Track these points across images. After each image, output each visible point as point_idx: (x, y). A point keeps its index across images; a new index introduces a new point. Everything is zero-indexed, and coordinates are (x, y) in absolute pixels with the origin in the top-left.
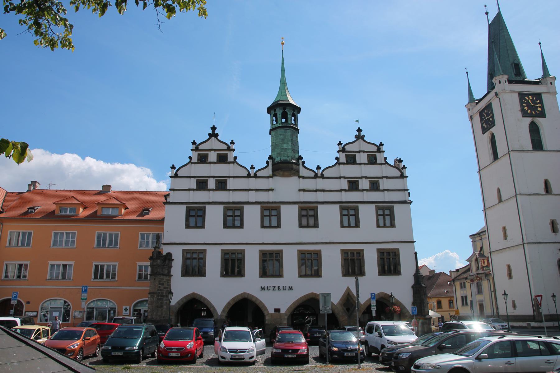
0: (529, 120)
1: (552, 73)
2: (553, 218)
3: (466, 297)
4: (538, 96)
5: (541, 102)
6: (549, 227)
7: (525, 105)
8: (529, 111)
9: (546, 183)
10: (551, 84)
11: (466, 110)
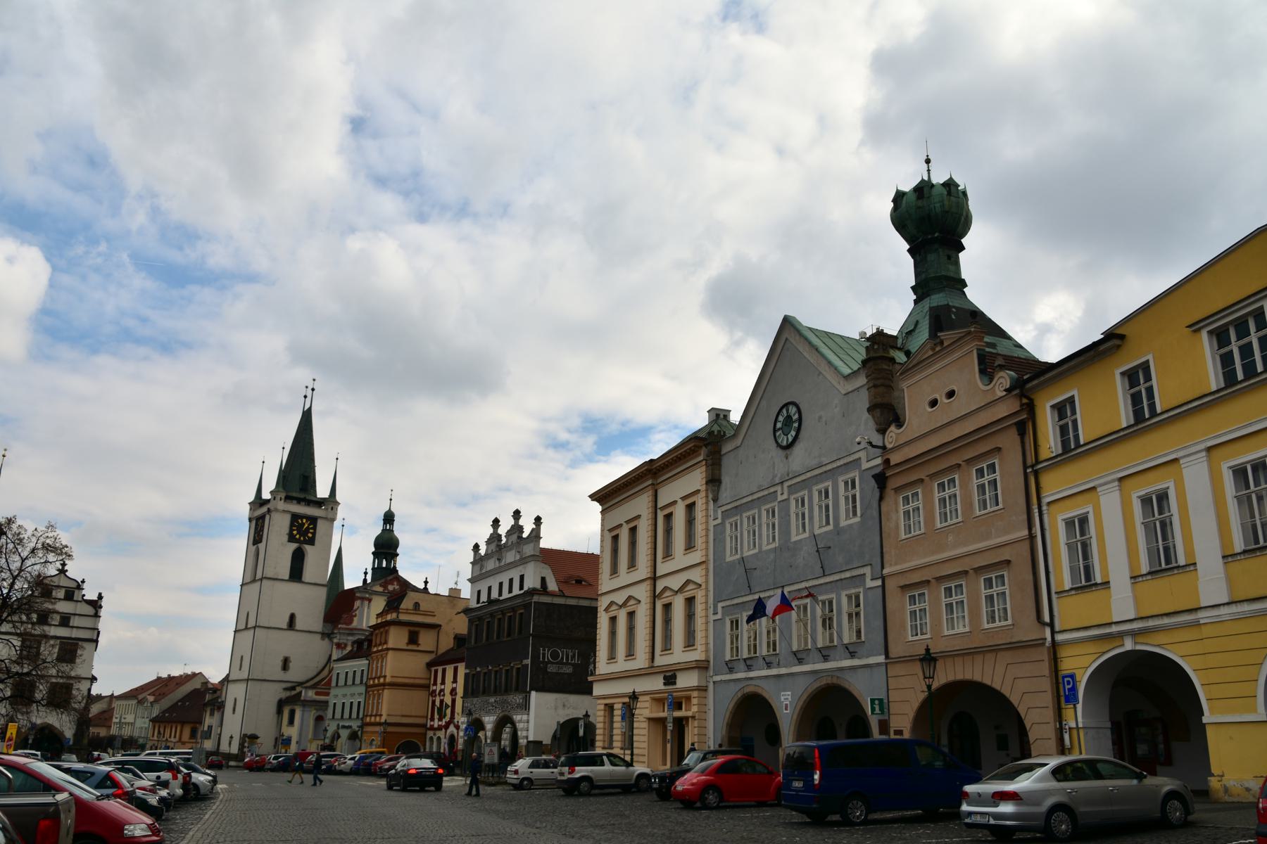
0: (294, 546)
1: (338, 498)
2: (287, 655)
3: (212, 726)
4: (313, 520)
5: (315, 528)
6: (280, 664)
7: (295, 528)
8: (298, 536)
9: (292, 617)
10: (332, 509)
11: (248, 507)
